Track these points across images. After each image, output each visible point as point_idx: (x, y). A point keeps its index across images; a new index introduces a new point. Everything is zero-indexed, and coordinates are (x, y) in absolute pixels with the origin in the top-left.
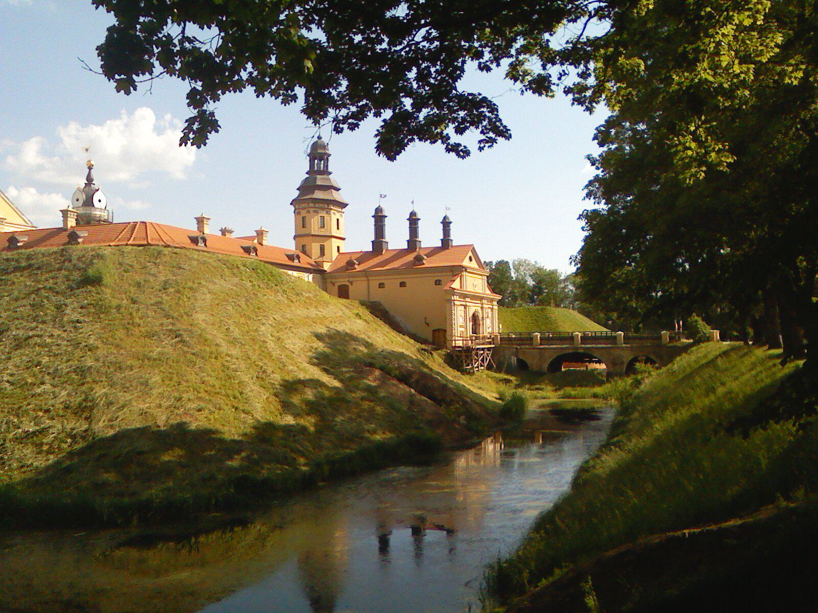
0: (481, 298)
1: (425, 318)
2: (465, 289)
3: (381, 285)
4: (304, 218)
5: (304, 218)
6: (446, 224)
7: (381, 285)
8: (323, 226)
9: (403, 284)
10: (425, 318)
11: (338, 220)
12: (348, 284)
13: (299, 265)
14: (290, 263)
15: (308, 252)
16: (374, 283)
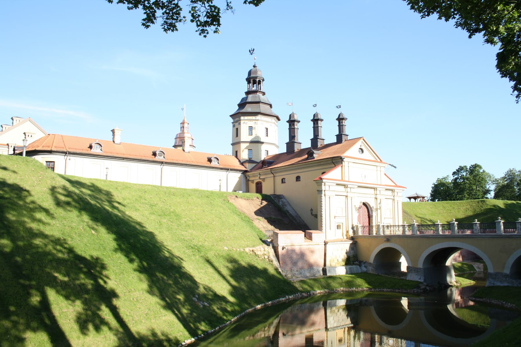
0: (375, 189)
1: (312, 210)
2: (347, 179)
3: (283, 181)
4: (237, 129)
5: (237, 129)
6: (340, 119)
7: (283, 181)
8: (251, 134)
9: (298, 178)
10: (312, 210)
11: (267, 129)
12: (260, 180)
13: (218, 165)
14: (208, 164)
15: (238, 157)
16: (279, 180)
